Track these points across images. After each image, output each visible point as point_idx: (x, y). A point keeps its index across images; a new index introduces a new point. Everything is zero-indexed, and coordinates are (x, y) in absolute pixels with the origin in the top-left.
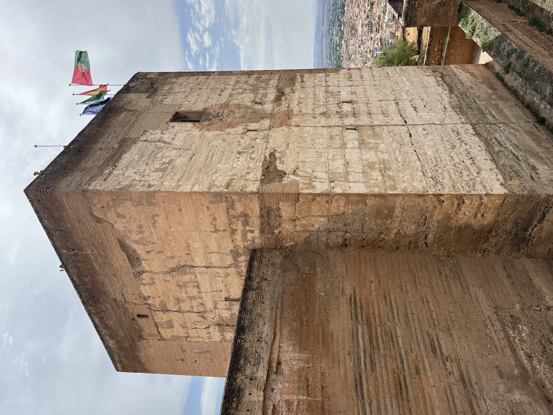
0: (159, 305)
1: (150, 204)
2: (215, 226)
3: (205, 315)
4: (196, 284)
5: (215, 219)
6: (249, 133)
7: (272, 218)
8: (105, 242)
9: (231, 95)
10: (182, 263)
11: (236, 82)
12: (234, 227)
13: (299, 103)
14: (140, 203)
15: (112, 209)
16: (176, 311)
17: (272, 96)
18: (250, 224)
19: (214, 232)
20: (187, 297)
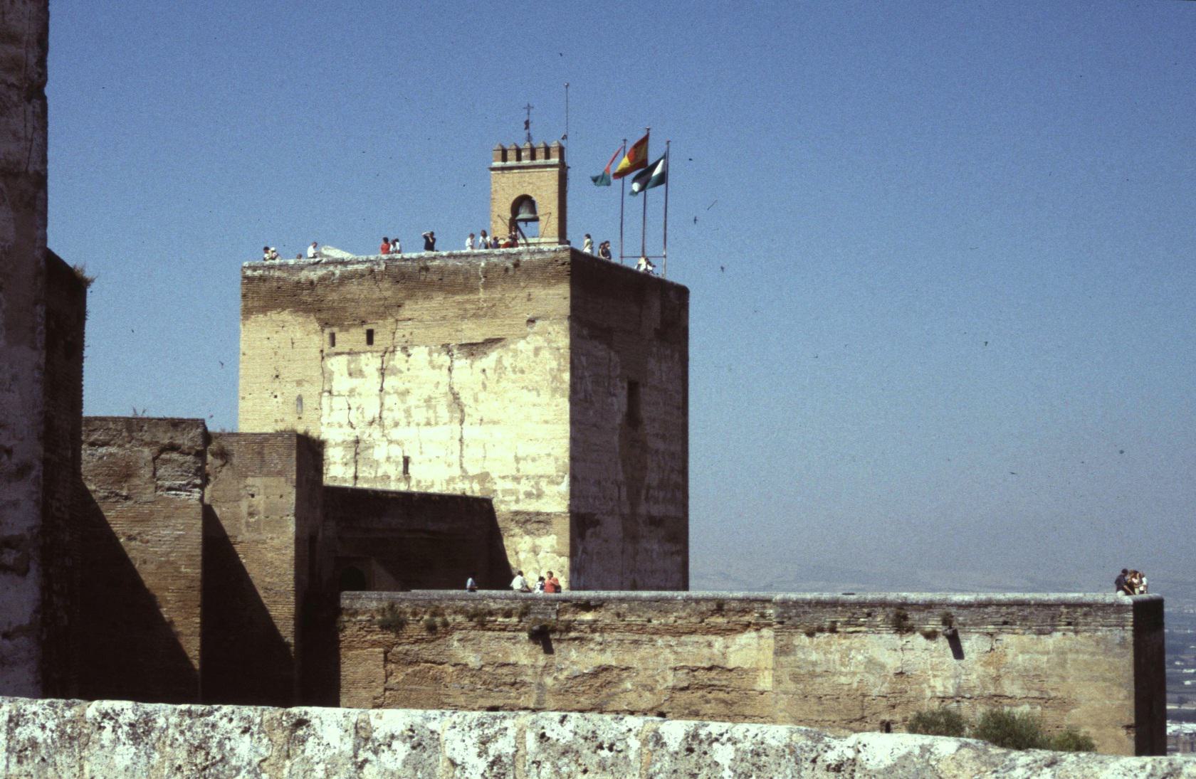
0: (394, 366)
1: (555, 390)
2: (525, 459)
3: (375, 425)
4: (433, 422)
5: (534, 460)
6: (617, 488)
7: (535, 526)
8: (498, 321)
9: (657, 451)
10: (467, 410)
11: (673, 454)
12: (523, 481)
13: (646, 551)
14: (554, 378)
15: (546, 345)
16: (382, 387)
17: (656, 510)
18: (527, 500)
19: (516, 456)
20: (410, 407)
